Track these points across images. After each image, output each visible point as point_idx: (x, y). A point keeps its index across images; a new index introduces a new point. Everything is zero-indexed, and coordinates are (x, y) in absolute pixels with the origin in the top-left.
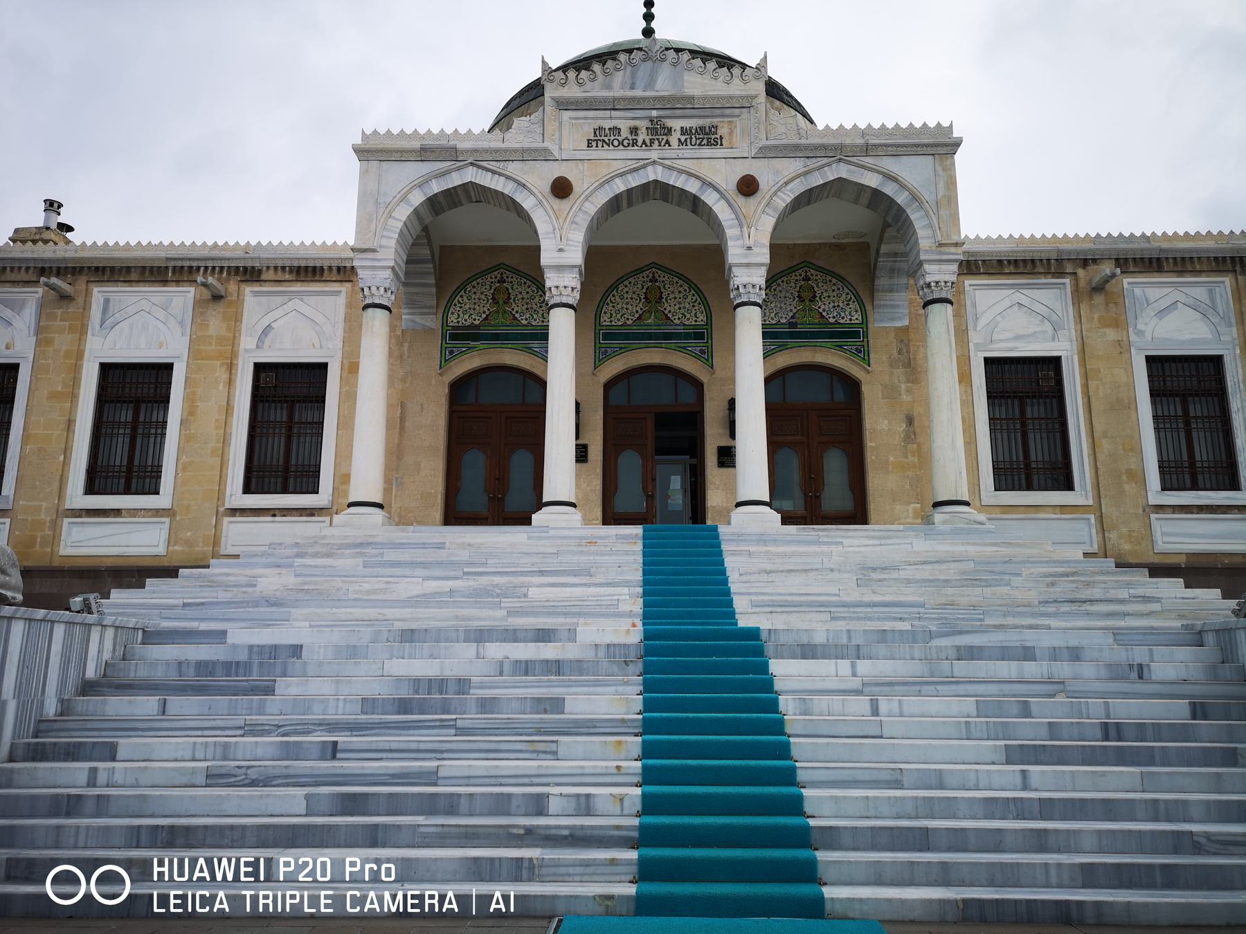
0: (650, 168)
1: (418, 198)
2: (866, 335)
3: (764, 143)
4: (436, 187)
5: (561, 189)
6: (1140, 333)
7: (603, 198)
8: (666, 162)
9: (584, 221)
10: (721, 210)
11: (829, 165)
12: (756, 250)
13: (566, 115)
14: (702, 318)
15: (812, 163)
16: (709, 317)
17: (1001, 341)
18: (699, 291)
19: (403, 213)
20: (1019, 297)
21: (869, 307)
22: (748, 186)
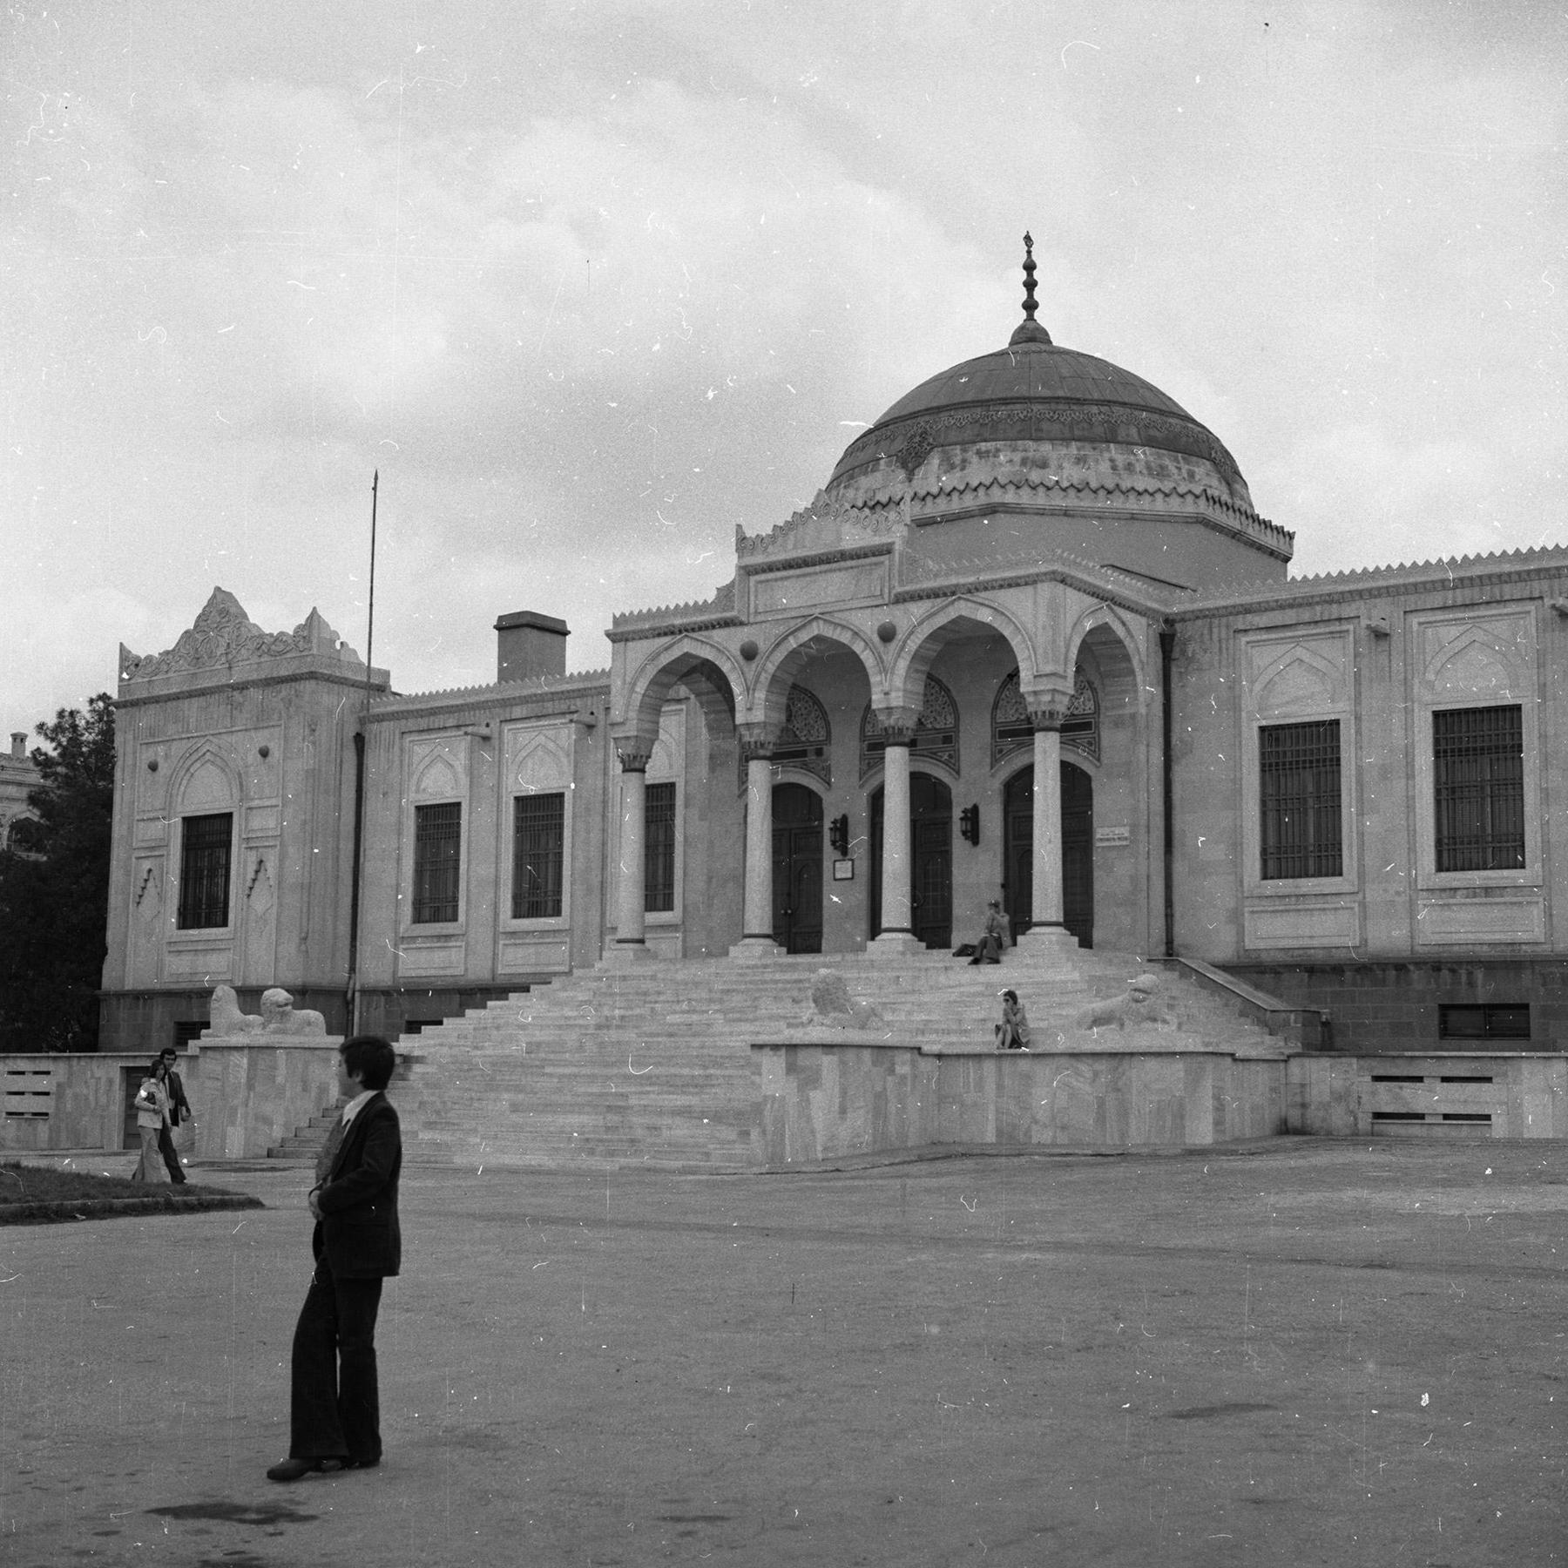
0: (814, 624)
1: (651, 671)
2: (1097, 727)
3: (899, 589)
4: (665, 659)
5: (749, 654)
6: (1430, 686)
7: (779, 656)
8: (827, 617)
9: (765, 678)
10: (868, 659)
11: (952, 602)
12: (893, 694)
13: (753, 579)
14: (950, 719)
15: (939, 602)
16: (957, 719)
17: (1278, 706)
18: (948, 691)
19: (641, 687)
20: (1300, 652)
21: (1101, 694)
22: (887, 635)
